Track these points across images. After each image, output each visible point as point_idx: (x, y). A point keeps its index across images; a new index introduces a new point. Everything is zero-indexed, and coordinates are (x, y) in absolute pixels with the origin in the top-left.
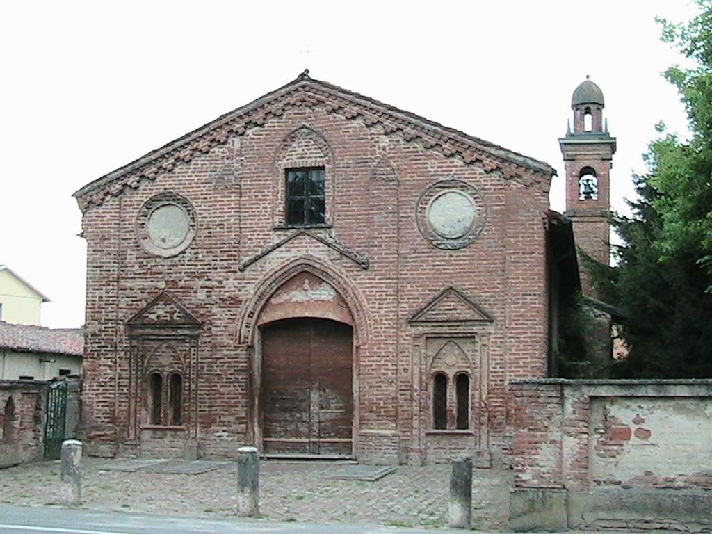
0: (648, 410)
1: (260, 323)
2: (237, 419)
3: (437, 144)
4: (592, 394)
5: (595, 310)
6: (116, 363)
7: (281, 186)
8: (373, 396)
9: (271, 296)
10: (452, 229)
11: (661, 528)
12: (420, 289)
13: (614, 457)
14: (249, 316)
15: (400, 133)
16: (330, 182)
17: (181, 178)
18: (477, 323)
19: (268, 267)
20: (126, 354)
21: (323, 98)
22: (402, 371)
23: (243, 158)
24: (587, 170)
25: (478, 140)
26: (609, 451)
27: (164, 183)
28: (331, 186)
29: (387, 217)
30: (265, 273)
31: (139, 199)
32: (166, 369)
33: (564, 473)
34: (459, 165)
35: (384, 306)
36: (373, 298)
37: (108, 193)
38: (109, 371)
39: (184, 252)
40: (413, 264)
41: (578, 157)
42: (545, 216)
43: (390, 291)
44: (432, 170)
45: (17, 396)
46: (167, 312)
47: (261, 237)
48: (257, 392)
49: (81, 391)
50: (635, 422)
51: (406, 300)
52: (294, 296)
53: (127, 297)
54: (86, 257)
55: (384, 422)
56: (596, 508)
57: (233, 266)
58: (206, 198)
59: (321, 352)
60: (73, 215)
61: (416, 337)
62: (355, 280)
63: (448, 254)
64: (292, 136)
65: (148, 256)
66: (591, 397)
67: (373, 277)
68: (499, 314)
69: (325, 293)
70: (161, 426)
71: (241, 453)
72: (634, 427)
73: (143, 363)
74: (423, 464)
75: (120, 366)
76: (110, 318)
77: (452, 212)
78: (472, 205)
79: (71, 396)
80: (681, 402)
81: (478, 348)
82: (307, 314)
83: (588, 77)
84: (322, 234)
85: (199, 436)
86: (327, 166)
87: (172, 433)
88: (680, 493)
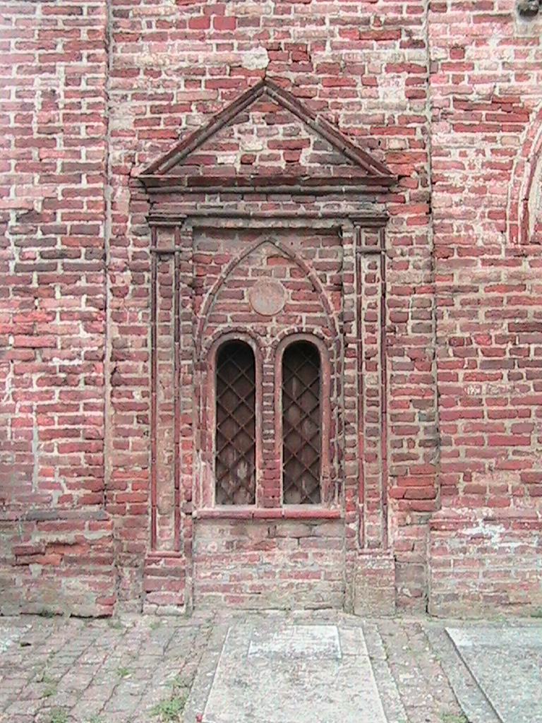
2: (525, 479)
32: (271, 326)
38: (84, 335)
46: (275, 145)
53: (135, 97)
85: (395, 536)
87: (301, 529)
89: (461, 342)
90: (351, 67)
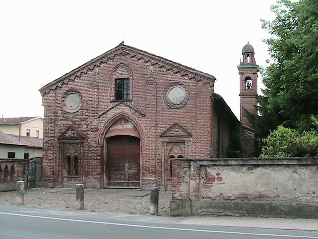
0: (222, 170)
1: (106, 137)
3: (171, 69)
4: (201, 164)
5: (249, 131)
6: (54, 152)
7: (113, 86)
8: (147, 164)
9: (109, 128)
10: (176, 101)
11: (225, 215)
12: (165, 124)
13: (209, 188)
14: (102, 135)
15: (157, 65)
16: (132, 83)
17: (77, 83)
18: (186, 137)
19: (109, 116)
20: (58, 149)
21: (129, 52)
22: (157, 155)
23: (99, 75)
24: (248, 78)
25: (186, 67)
26: (207, 185)
27: (71, 85)
28: (132, 85)
29: (152, 97)
30: (107, 118)
31: (62, 91)
33: (190, 194)
34: (179, 76)
35: (151, 130)
36: (147, 128)
37: (51, 90)
38: (51, 156)
39: (78, 111)
40: (162, 114)
41: (245, 73)
42: (211, 96)
43: (153, 125)
44: (169, 78)
45: (15, 165)
46: (72, 133)
47: (106, 105)
48: (105, 163)
49: (42, 163)
50: (217, 174)
51: (159, 128)
52: (118, 127)
54: (44, 113)
55: (151, 174)
56: (201, 207)
57: (96, 116)
58: (86, 91)
59: (128, 148)
60: (39, 97)
61: (163, 142)
62: (141, 121)
63: (175, 111)
64: (117, 67)
65: (66, 113)
66: (200, 165)
67: (147, 119)
68: (194, 133)
69: (130, 126)
70: (70, 176)
71: (77, 186)
72: (216, 177)
73: (64, 153)
74: (166, 190)
75: (56, 154)
76: (52, 136)
77: (177, 95)
78: (184, 92)
79: (38, 165)
80: (234, 167)
81: (186, 147)
82: (123, 134)
83: (248, 42)
84: (128, 104)
85: (84, 179)
86: (130, 78)
87: (75, 179)
88: (232, 202)
89: (91, 157)
90: (81, 124)
